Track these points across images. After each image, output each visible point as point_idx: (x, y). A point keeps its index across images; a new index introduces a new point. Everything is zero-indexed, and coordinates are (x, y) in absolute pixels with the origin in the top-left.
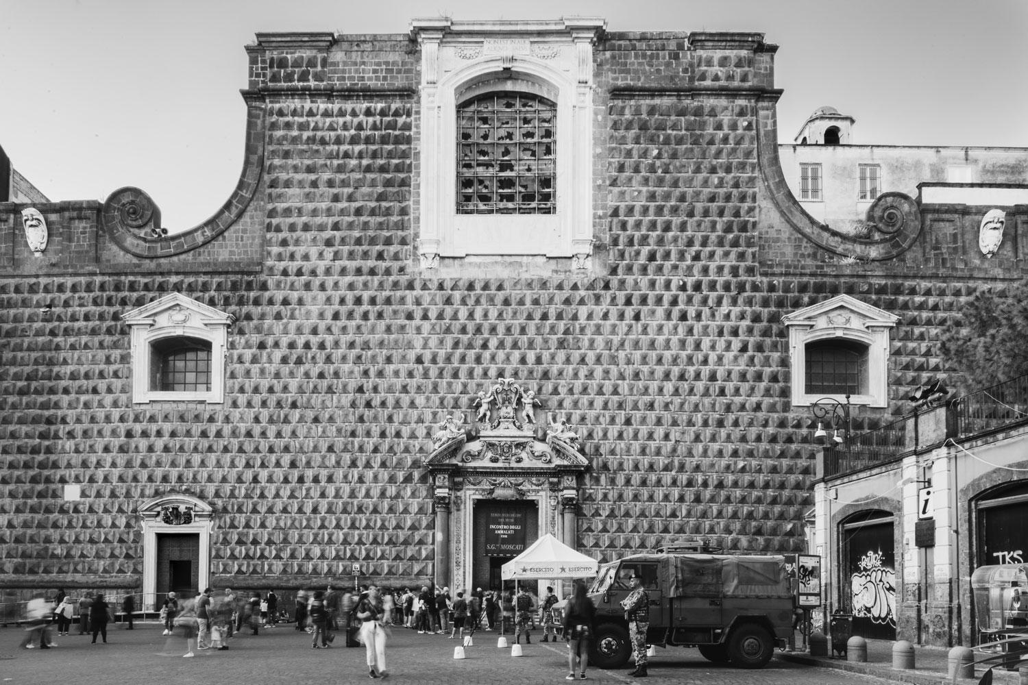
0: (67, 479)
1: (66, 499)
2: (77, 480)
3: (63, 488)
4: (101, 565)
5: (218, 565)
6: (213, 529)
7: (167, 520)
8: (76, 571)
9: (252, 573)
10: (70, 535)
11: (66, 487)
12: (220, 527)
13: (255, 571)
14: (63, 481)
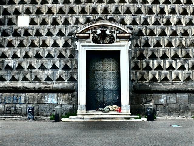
0: (20, 11)
1: (19, 26)
2: (28, 12)
3: (17, 18)
4: (43, 75)
5: (136, 74)
6: (130, 47)
7: (95, 41)
8: (25, 79)
9: (163, 80)
10: (20, 52)
11: (19, 17)
12: (137, 46)
13: (166, 79)
14: (17, 13)
